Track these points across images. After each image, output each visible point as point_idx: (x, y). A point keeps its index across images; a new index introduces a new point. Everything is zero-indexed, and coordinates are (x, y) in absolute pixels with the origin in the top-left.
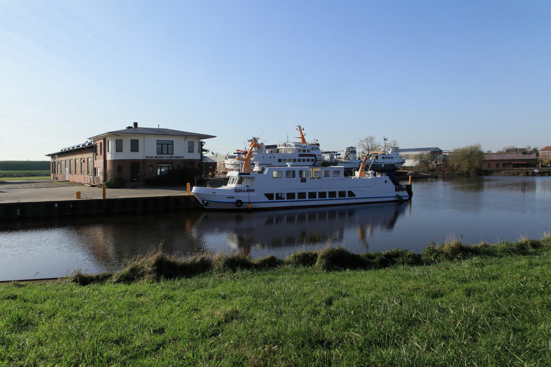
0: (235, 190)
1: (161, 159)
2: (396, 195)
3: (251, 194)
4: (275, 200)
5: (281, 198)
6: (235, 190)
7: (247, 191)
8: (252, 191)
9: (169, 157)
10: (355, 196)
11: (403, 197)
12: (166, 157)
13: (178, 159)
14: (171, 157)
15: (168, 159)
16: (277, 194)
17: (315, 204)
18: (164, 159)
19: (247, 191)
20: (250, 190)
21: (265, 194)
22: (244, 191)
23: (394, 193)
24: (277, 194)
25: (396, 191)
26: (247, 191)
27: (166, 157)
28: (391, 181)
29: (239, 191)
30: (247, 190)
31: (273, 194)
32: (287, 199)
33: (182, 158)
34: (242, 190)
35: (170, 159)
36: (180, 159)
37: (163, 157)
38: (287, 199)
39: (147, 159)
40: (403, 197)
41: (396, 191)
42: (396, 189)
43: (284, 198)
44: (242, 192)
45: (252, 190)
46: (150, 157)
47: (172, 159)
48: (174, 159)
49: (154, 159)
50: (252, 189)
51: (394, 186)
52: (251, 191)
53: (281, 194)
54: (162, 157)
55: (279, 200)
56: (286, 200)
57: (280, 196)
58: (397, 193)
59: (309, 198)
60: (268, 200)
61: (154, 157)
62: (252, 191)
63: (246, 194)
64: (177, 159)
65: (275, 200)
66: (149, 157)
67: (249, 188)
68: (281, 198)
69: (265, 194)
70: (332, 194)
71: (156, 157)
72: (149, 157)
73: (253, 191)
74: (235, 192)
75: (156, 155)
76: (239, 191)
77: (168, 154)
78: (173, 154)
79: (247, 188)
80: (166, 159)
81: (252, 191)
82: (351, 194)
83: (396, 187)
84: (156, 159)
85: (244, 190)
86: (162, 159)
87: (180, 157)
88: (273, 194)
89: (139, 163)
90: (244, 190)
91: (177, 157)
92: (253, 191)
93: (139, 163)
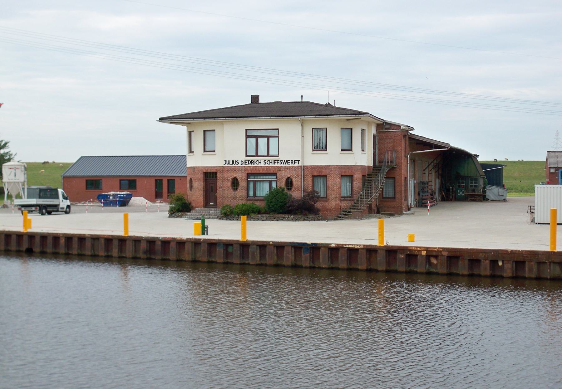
1: (252, 165)
9: (268, 162)
12: (263, 163)
13: (287, 165)
14: (273, 162)
15: (267, 165)
18: (260, 165)
27: (263, 163)
33: (296, 164)
35: (271, 165)
36: (292, 165)
37: (257, 163)
39: (226, 165)
46: (233, 161)
47: (276, 164)
48: (279, 165)
49: (240, 165)
54: (256, 162)
61: (240, 162)
64: (285, 165)
66: (231, 163)
71: (244, 162)
72: (231, 163)
75: (244, 158)
77: (268, 155)
78: (277, 156)
80: (263, 165)
84: (243, 165)
86: (256, 165)
87: (292, 162)
89: (215, 173)
91: (284, 162)
93: (215, 173)
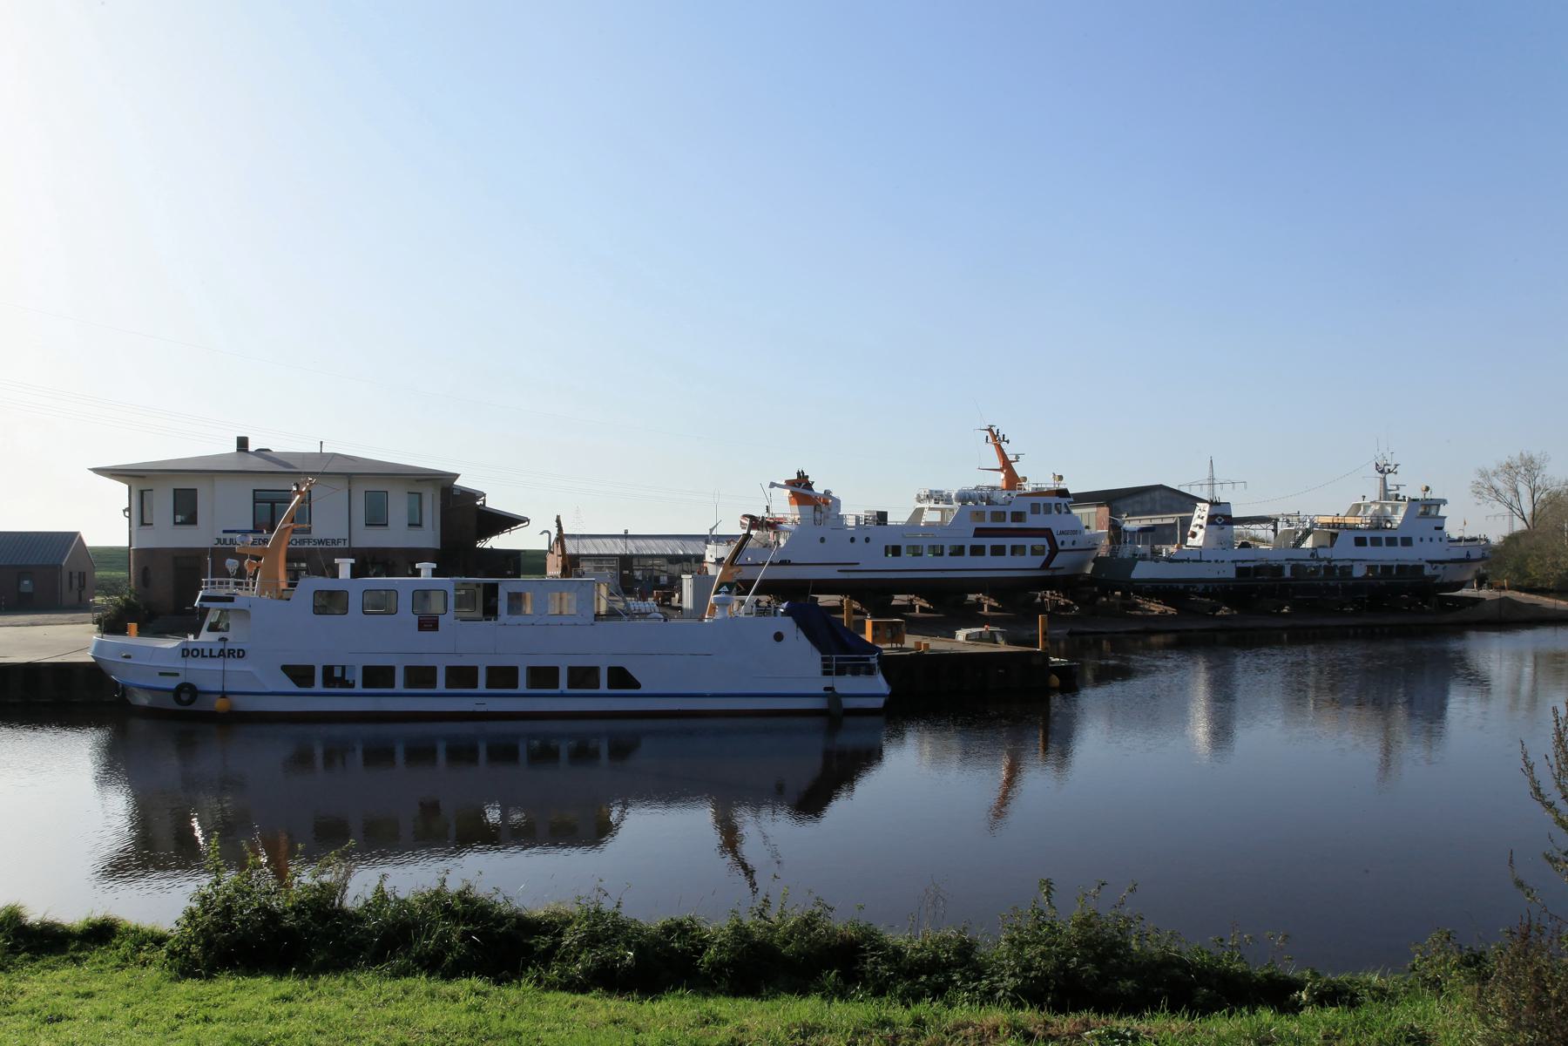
0: (183, 650)
2: (826, 689)
3: (233, 665)
4: (318, 686)
5: (343, 682)
6: (183, 650)
7: (222, 653)
8: (239, 656)
10: (638, 686)
11: (843, 699)
16: (328, 670)
17: (471, 710)
19: (219, 655)
20: (229, 650)
21: (285, 668)
22: (211, 656)
23: (819, 684)
24: (328, 670)
25: (825, 673)
26: (219, 655)
28: (801, 634)
29: (195, 653)
30: (222, 650)
31: (312, 668)
32: (365, 686)
34: (203, 650)
38: (365, 686)
40: (843, 699)
41: (825, 673)
42: (825, 666)
43: (354, 681)
44: (203, 656)
45: (239, 650)
50: (236, 647)
51: (818, 656)
52: (234, 657)
53: (344, 668)
55: (334, 687)
56: (358, 688)
57: (338, 673)
58: (828, 681)
59: (447, 686)
60: (292, 687)
62: (236, 654)
63: (216, 665)
65: (318, 686)
67: (229, 646)
68: (343, 682)
69: (285, 668)
70: (543, 677)
73: (241, 654)
74: (183, 656)
76: (195, 653)
79: (221, 646)
81: (236, 654)
82: (621, 678)
83: (823, 659)
85: (211, 650)
88: (312, 668)
90: (211, 650)
92: (241, 654)
